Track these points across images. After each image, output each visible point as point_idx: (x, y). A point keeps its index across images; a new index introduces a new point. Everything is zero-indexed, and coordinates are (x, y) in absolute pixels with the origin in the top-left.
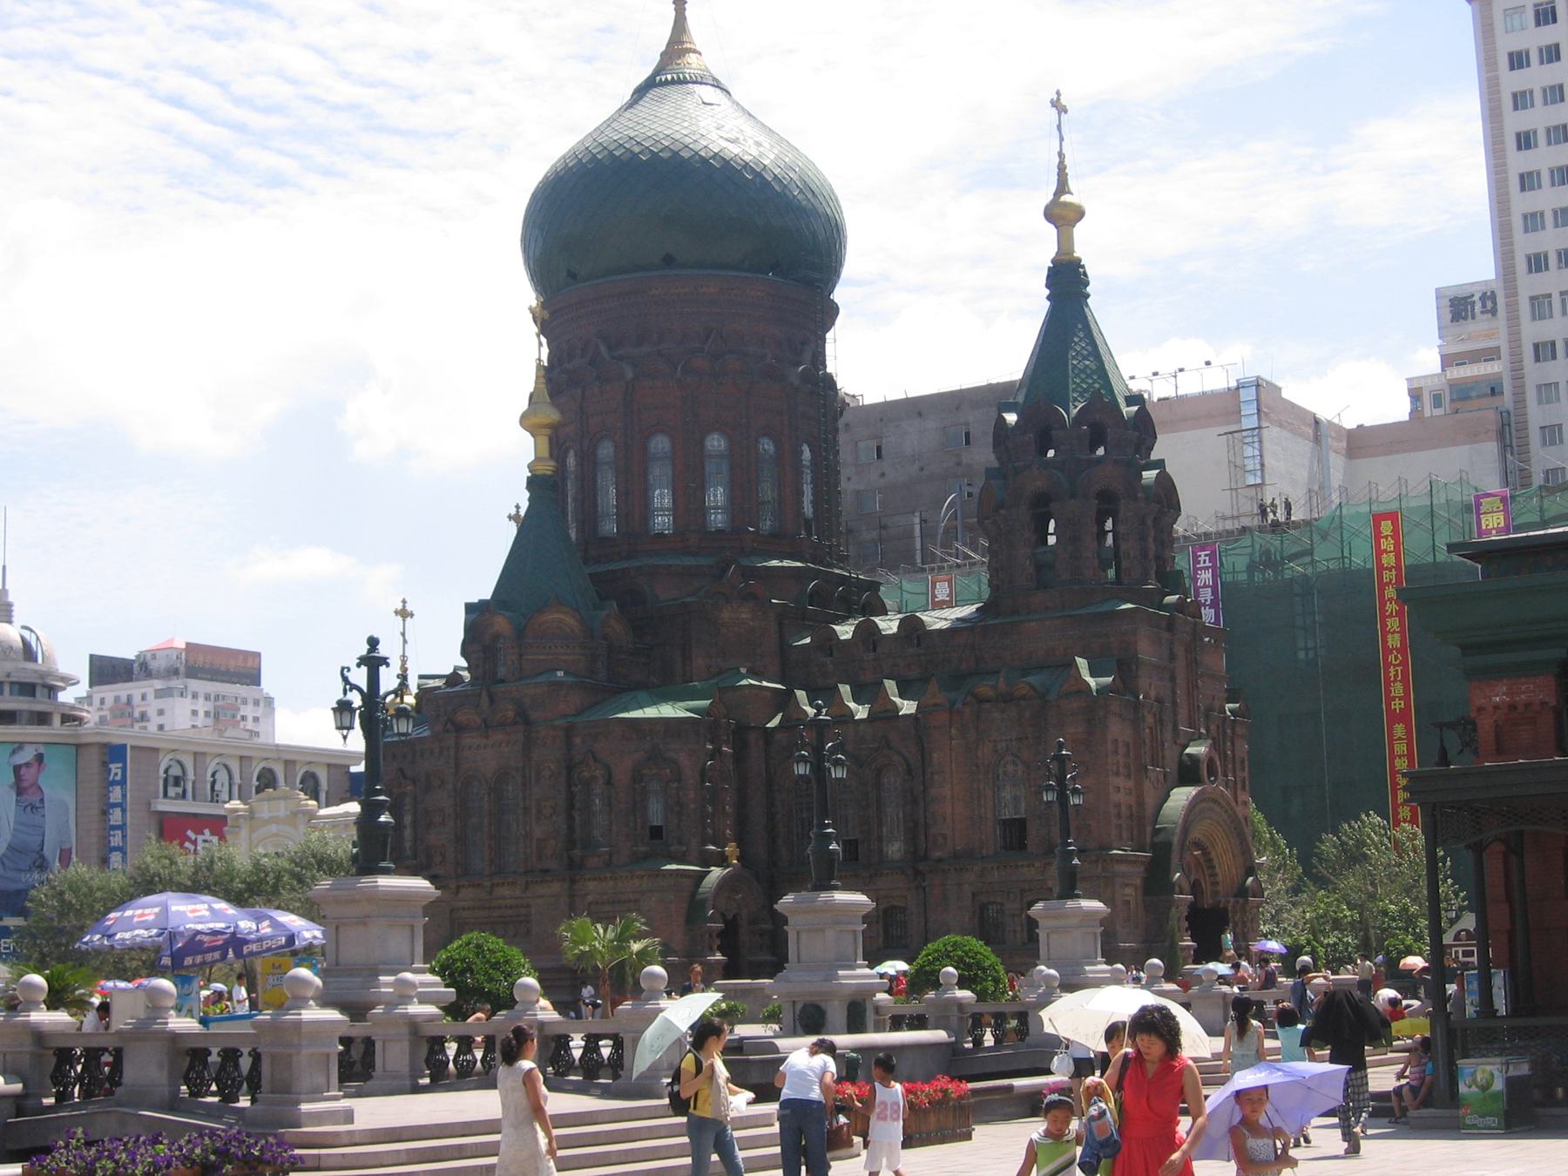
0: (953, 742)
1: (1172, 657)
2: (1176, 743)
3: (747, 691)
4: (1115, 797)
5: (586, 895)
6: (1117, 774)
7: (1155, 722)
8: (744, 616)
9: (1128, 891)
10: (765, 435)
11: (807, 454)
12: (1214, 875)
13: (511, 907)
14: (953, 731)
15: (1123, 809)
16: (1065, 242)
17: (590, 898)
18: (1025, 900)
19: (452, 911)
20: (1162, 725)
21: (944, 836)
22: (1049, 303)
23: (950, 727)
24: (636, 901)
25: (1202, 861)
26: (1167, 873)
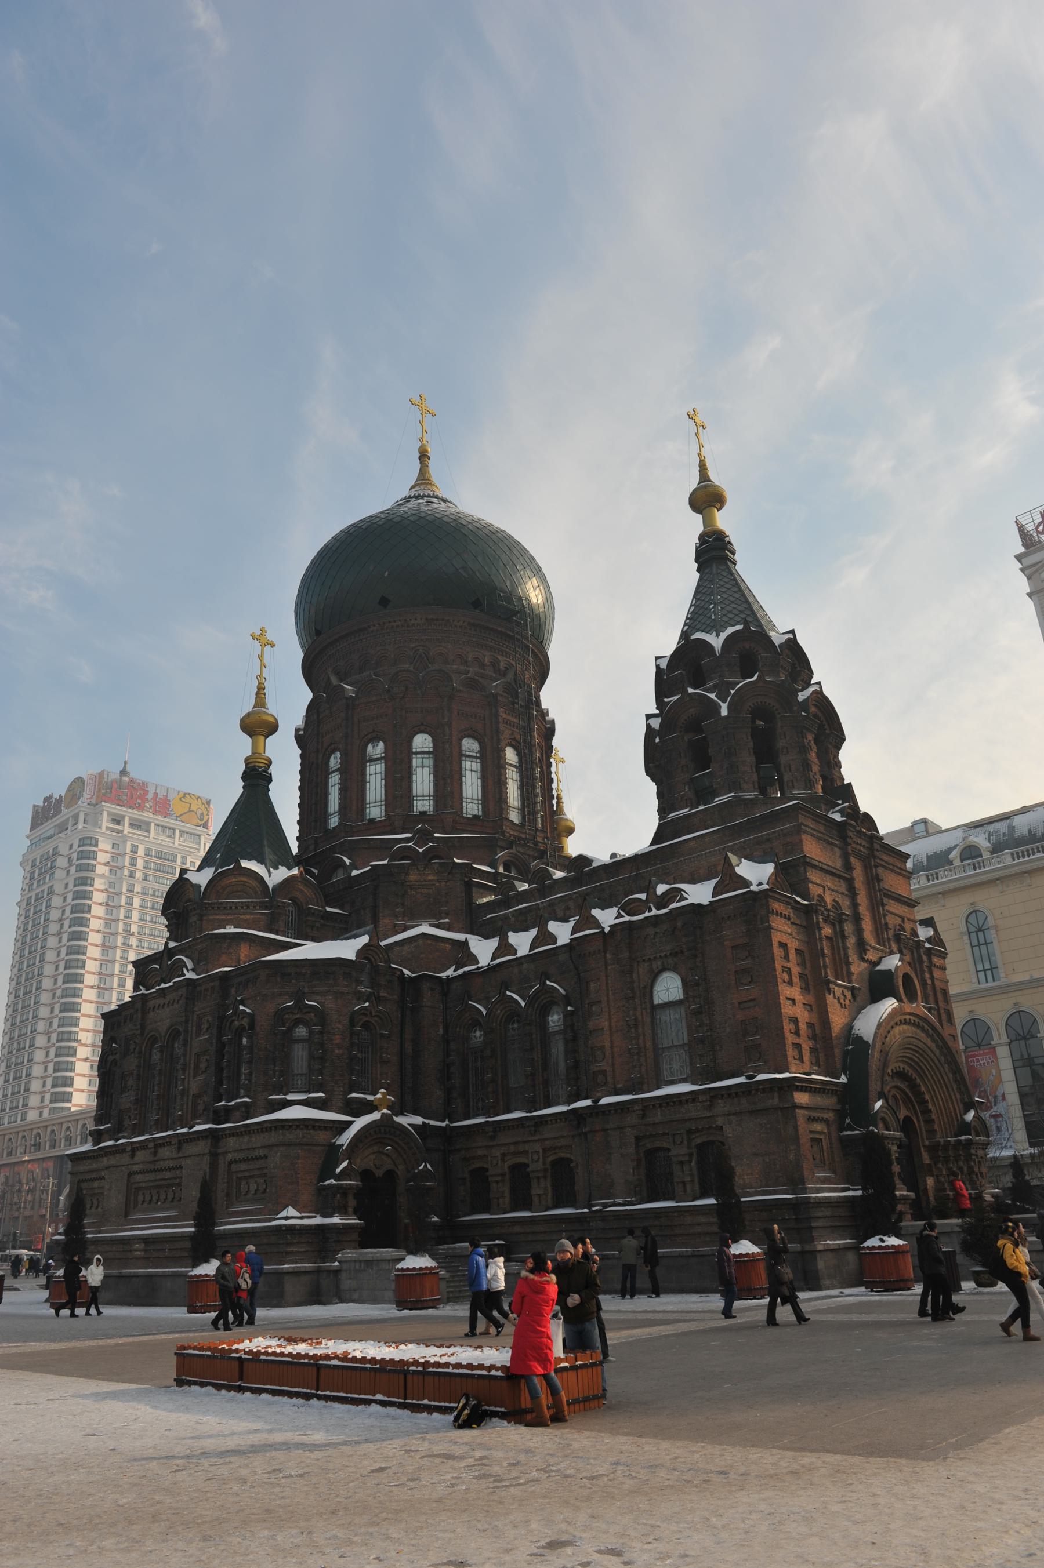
0: (609, 968)
1: (848, 867)
2: (863, 959)
3: (421, 942)
4: (787, 1010)
5: (226, 1153)
6: (790, 983)
7: (835, 933)
8: (430, 878)
9: (818, 1127)
10: (469, 736)
11: (511, 755)
12: (927, 1112)
13: (169, 1169)
14: (608, 956)
15: (803, 1026)
16: (708, 521)
17: (230, 1156)
18: (693, 1144)
19: (130, 1175)
20: (844, 937)
21: (604, 1073)
22: (699, 575)
23: (605, 952)
24: (266, 1157)
25: (908, 1091)
26: (867, 1104)
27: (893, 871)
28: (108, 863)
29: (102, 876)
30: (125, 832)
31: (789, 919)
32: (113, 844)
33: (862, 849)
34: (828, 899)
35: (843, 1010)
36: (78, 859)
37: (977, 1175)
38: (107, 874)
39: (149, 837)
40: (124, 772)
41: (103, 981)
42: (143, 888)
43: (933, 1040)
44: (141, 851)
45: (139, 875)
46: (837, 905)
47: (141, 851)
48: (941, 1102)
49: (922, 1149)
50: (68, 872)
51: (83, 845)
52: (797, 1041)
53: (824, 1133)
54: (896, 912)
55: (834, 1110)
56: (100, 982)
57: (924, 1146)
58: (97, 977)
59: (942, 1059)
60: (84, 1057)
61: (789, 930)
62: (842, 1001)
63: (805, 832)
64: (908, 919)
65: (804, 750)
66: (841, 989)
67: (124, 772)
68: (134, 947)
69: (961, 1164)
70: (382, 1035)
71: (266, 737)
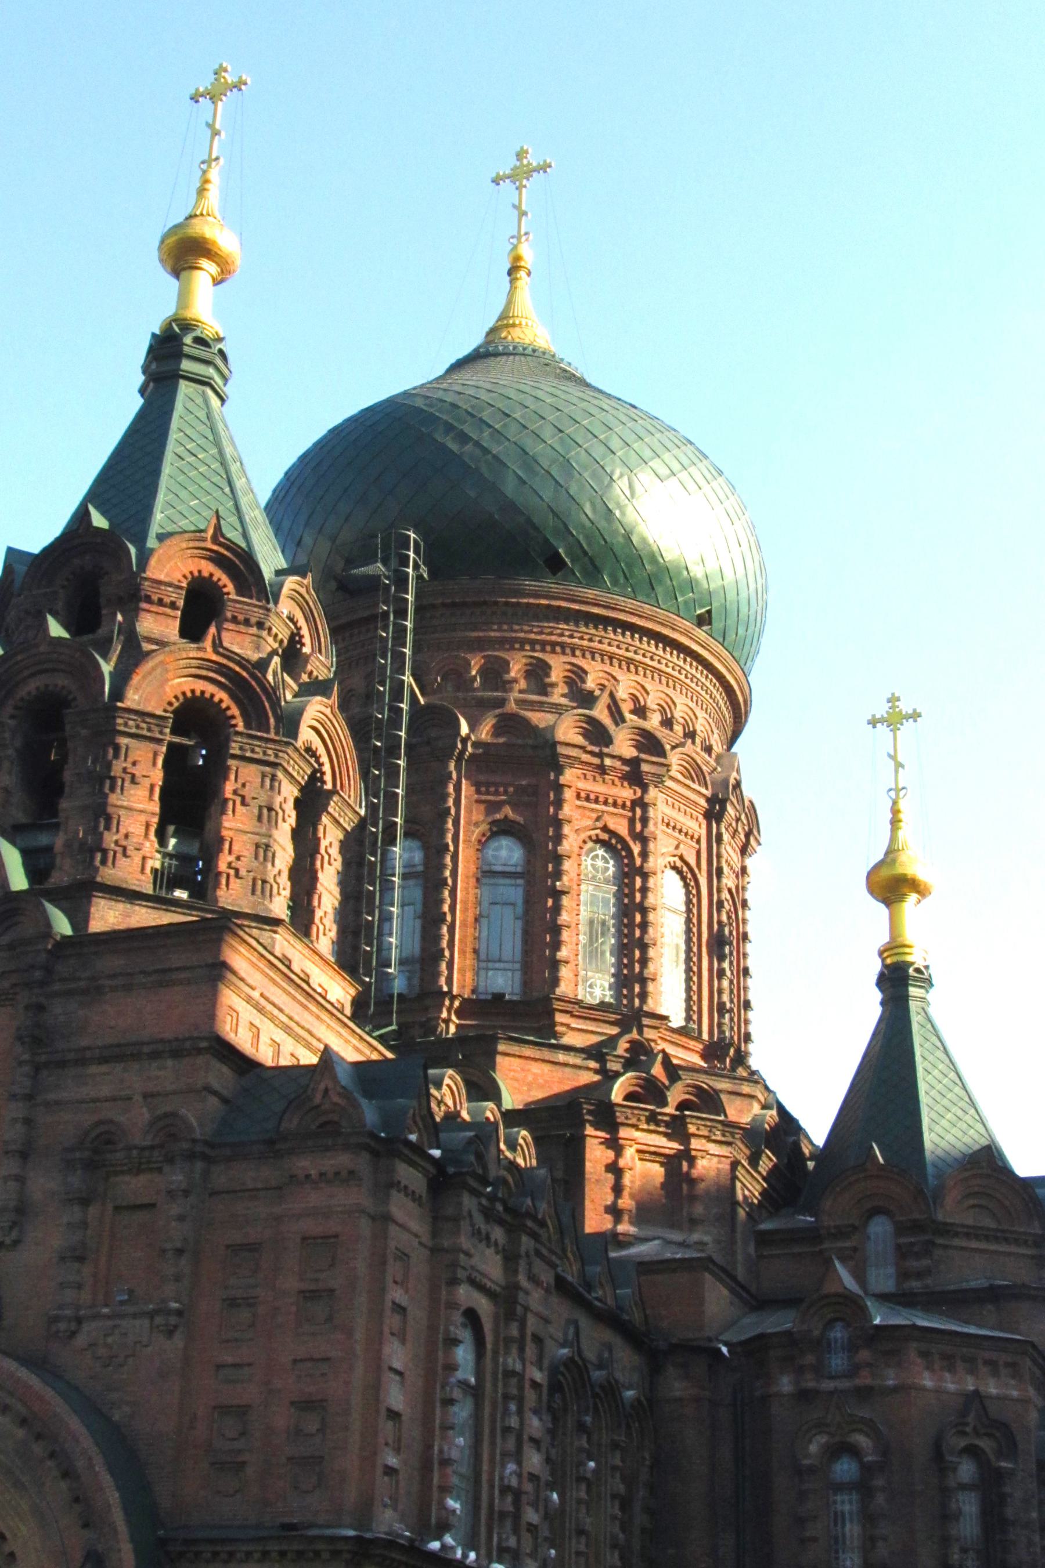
27: (128, 988)
54: (105, 1091)
59: (38, 1449)
64: (146, 1096)
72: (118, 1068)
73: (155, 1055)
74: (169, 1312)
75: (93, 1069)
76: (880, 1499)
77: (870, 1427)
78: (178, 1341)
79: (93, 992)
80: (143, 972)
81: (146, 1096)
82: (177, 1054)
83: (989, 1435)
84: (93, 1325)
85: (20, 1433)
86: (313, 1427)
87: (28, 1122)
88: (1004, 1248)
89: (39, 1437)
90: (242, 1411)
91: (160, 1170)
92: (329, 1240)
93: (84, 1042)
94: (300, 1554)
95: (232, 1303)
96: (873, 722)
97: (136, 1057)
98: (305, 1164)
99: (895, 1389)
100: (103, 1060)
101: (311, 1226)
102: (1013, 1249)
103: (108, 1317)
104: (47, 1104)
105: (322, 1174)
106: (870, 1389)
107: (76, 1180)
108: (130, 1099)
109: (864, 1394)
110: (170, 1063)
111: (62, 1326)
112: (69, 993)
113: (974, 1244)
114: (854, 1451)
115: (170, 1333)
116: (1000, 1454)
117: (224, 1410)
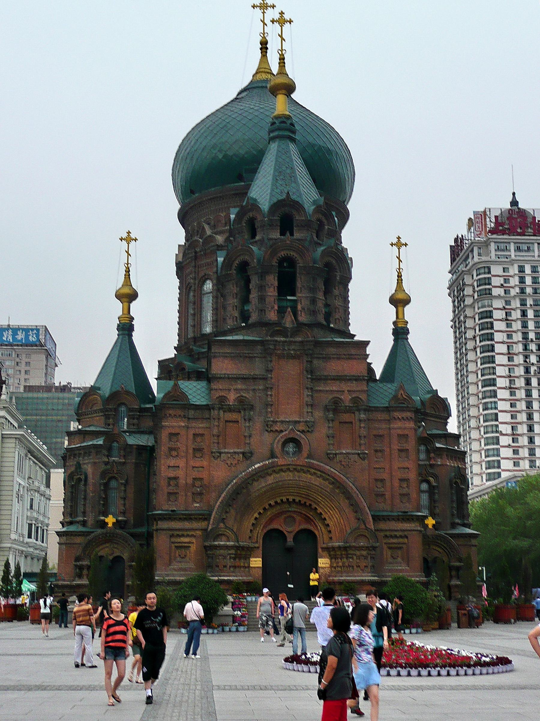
2: (267, 431)
9: (187, 540)
27: (338, 359)
28: (502, 285)
29: (499, 297)
30: (513, 257)
31: (184, 417)
32: (504, 268)
33: (292, 352)
34: (232, 397)
35: (229, 468)
36: (477, 287)
37: (353, 567)
38: (503, 294)
39: (534, 256)
40: (514, 203)
41: (513, 382)
42: (534, 301)
43: (324, 479)
44: (528, 270)
45: (529, 290)
46: (241, 401)
47: (528, 270)
48: (335, 519)
49: (320, 550)
50: (474, 297)
51: (480, 274)
52: (175, 491)
53: (193, 543)
55: (201, 530)
56: (510, 383)
57: (322, 548)
58: (507, 380)
59: (337, 491)
60: (507, 444)
61: (183, 424)
62: (229, 462)
63: (215, 357)
65: (261, 288)
66: (229, 455)
67: (514, 203)
68: (534, 351)
69: (345, 560)
70: (122, 484)
71: (130, 302)
72: (338, 382)
73: (350, 380)
74: (366, 453)
75: (329, 382)
76: (436, 497)
77: (435, 476)
78: (366, 461)
79: (327, 358)
80: (344, 355)
81: (348, 391)
82: (356, 380)
83: (460, 479)
84: (340, 456)
85: (331, 486)
86: (405, 486)
87: (312, 396)
88: (438, 420)
89: (338, 487)
90: (382, 481)
91: (354, 413)
92: (406, 436)
93: (325, 374)
94: (408, 519)
95: (376, 451)
96: (392, 245)
97: (344, 380)
98: (397, 414)
99: (440, 465)
100: (334, 379)
101: (400, 432)
102: (440, 420)
103: (345, 454)
104: (317, 391)
105: (403, 418)
106: (434, 465)
107: (331, 415)
108: (344, 391)
109: (431, 466)
110: (354, 382)
111: (331, 456)
112: (319, 358)
113: (432, 419)
114: (428, 482)
115: (363, 459)
116: (462, 484)
117: (376, 480)
